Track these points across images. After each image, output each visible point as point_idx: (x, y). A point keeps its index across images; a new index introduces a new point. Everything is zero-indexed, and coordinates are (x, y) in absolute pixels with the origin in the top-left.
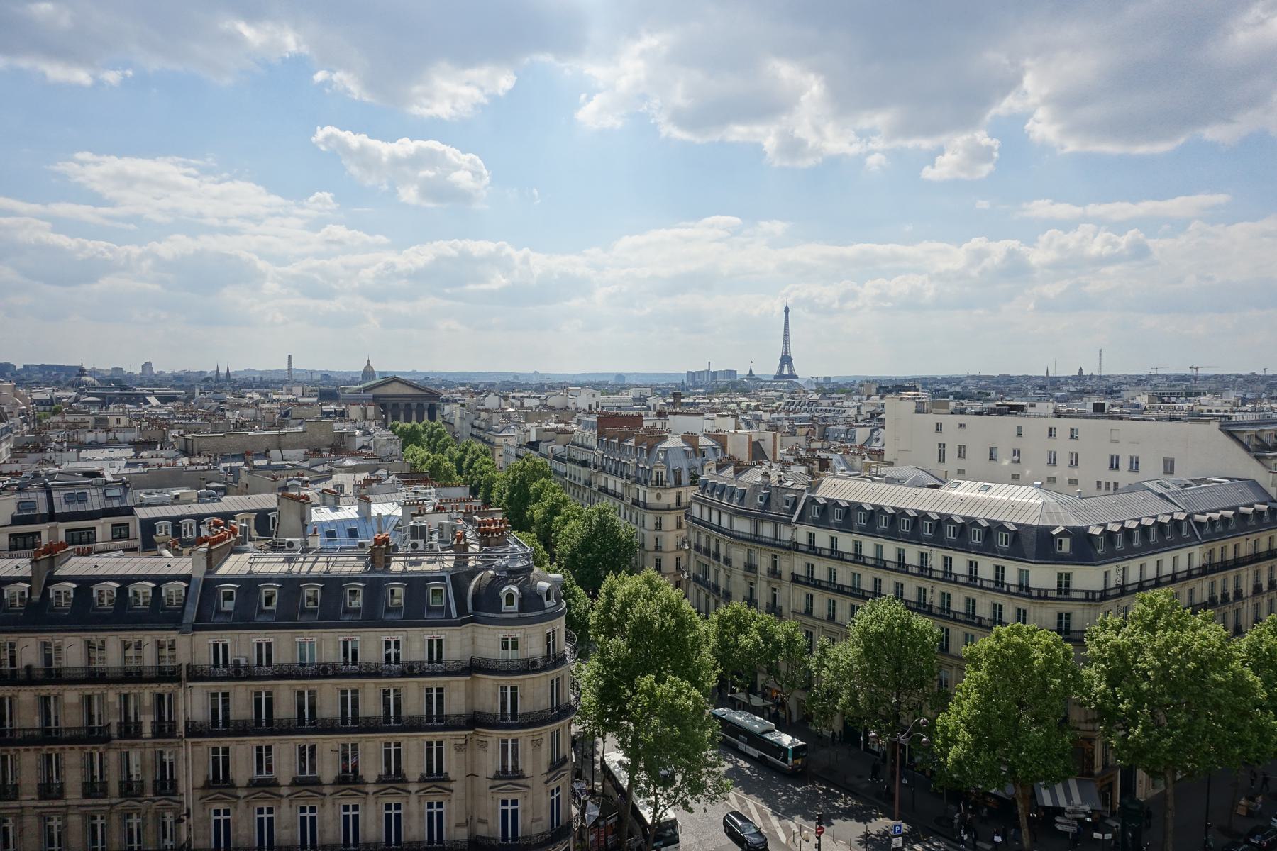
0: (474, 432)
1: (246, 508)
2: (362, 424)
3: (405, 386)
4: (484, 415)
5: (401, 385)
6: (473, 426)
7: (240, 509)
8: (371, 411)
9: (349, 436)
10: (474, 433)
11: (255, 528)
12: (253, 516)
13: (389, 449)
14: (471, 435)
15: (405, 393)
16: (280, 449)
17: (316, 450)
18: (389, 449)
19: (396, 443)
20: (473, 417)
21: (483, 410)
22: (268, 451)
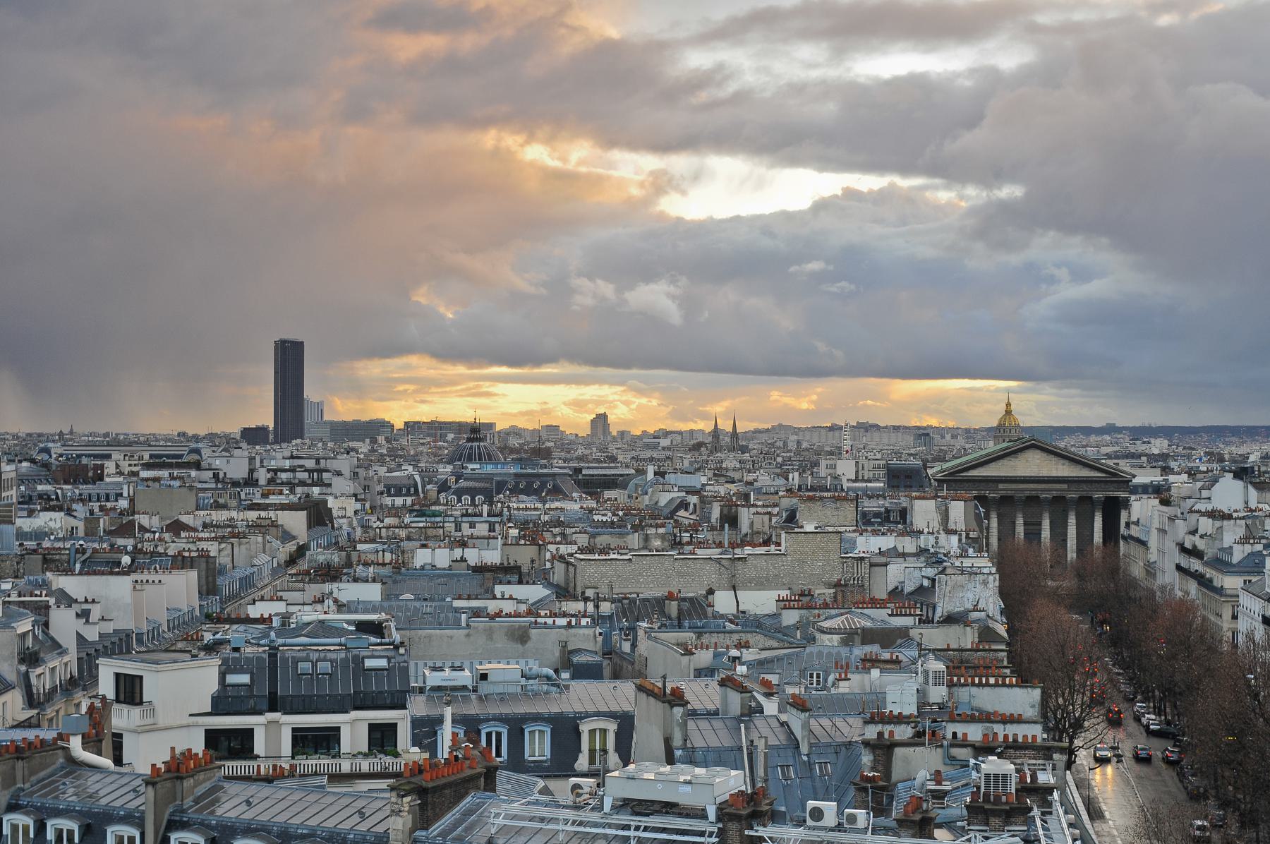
0: (1185, 562)
1: (604, 709)
2: (932, 539)
3: (1054, 459)
4: (1206, 525)
5: (1045, 455)
6: (1183, 549)
7: (591, 709)
8: (957, 510)
9: (872, 565)
10: (1184, 564)
11: (616, 750)
12: (612, 727)
13: (970, 595)
14: (1179, 567)
15: (1054, 474)
16: (734, 588)
17: (802, 594)
18: (970, 595)
19: (985, 583)
20: (1181, 527)
21: (1203, 514)
22: (711, 592)
